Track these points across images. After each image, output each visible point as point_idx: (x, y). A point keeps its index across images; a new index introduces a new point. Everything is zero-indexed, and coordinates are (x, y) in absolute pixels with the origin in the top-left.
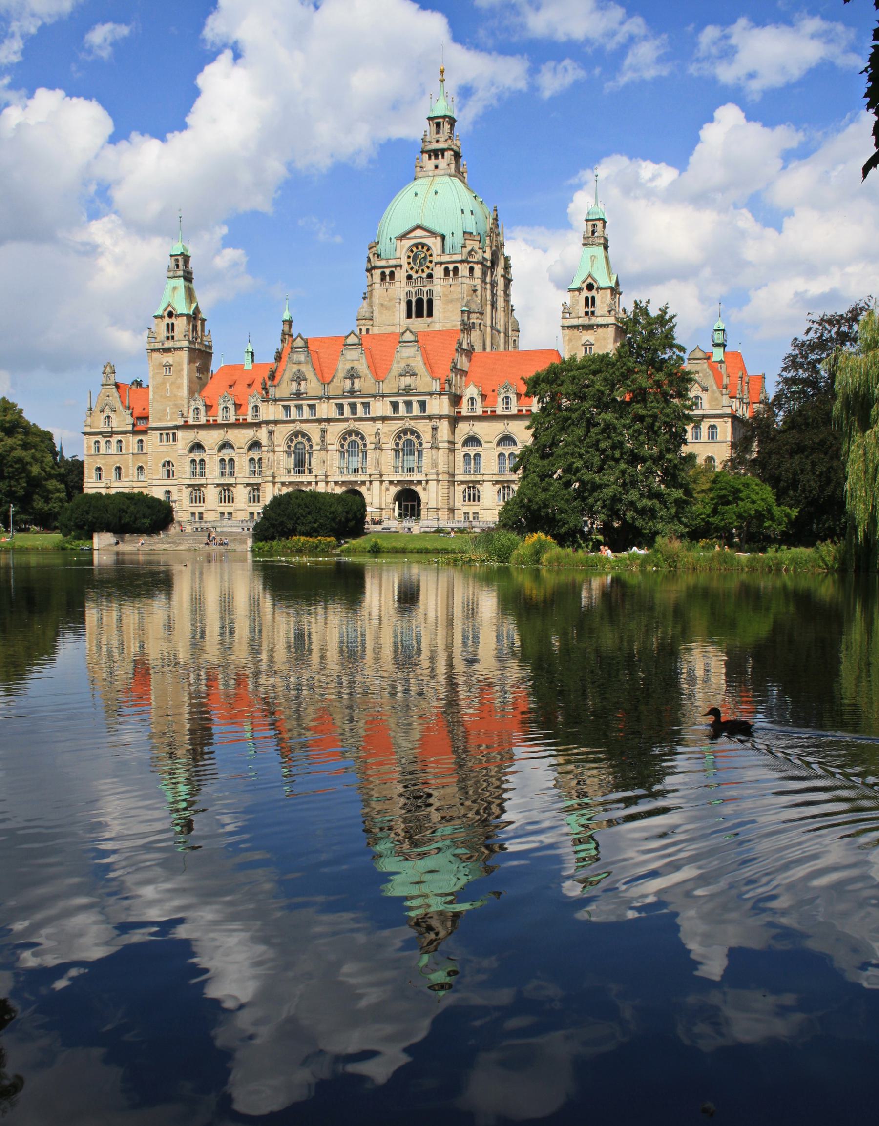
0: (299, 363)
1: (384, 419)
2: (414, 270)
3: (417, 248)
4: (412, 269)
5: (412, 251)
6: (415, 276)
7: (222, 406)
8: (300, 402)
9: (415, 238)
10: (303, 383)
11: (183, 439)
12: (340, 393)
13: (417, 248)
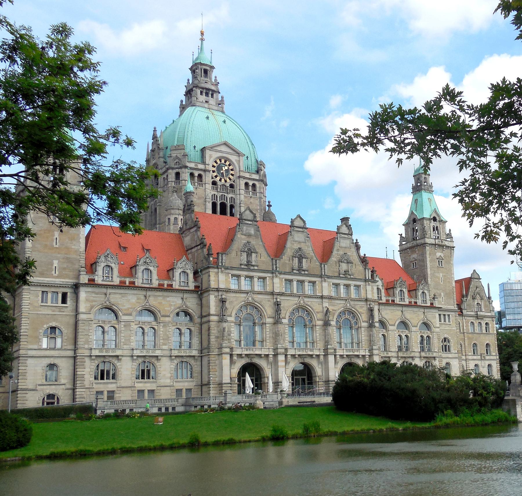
0: (249, 235)
1: (330, 298)
2: (218, 178)
3: (220, 161)
4: (216, 176)
5: (216, 162)
6: (219, 183)
7: (143, 268)
8: (251, 274)
9: (220, 151)
10: (254, 255)
11: (87, 300)
12: (288, 270)
13: (220, 161)
